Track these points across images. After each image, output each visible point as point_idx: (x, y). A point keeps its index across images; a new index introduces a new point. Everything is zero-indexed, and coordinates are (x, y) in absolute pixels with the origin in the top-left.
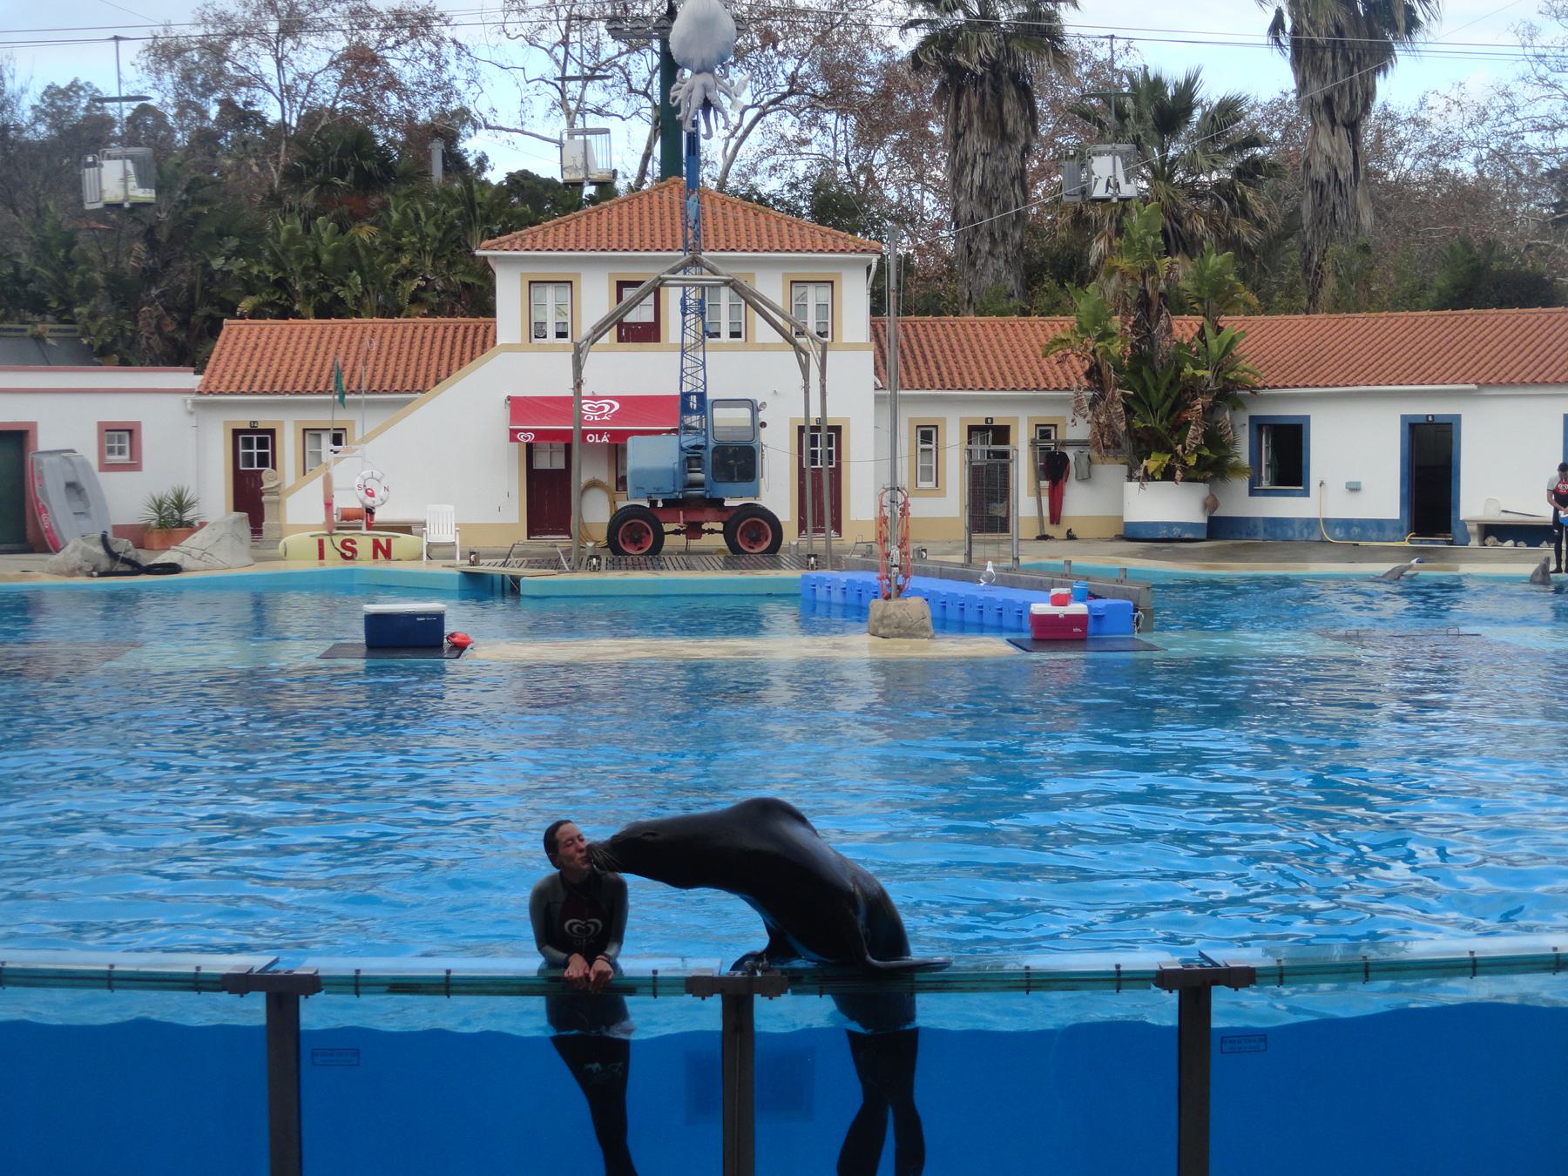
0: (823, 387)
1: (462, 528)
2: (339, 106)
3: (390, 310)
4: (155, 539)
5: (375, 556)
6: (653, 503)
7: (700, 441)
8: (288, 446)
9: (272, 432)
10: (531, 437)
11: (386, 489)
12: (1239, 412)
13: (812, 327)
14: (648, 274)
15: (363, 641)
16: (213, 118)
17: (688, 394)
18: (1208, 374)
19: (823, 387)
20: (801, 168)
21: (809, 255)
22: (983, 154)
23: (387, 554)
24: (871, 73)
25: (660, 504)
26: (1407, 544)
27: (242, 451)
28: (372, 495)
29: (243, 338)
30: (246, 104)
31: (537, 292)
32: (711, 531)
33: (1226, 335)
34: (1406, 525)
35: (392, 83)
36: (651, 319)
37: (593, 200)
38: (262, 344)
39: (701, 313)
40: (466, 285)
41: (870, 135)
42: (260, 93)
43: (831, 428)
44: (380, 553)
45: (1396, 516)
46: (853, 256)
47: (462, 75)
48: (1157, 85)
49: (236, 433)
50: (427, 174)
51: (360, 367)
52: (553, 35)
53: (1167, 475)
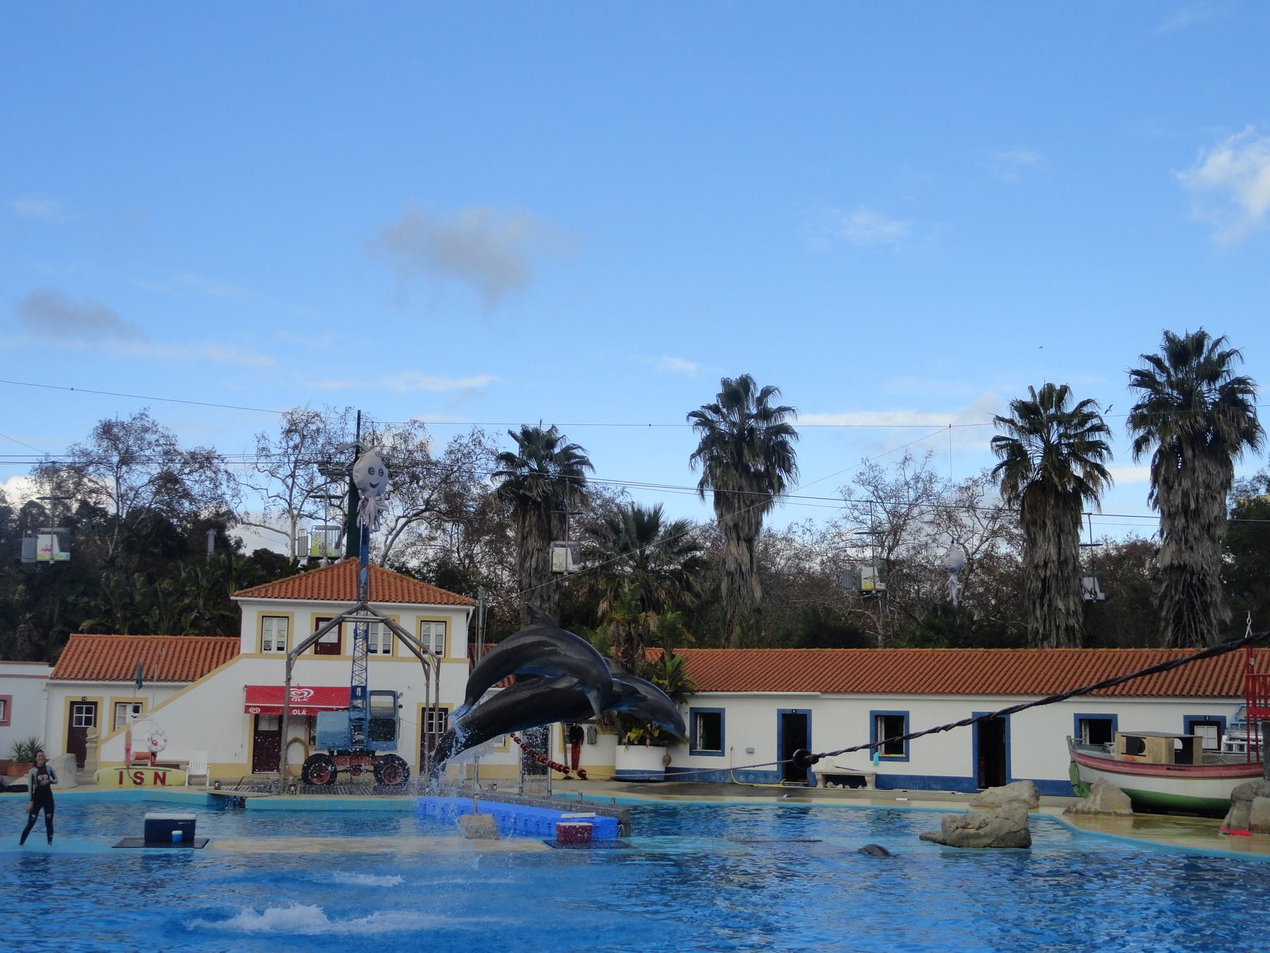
0: (437, 684)
1: (211, 766)
2: (153, 507)
3: (176, 630)
4: (14, 770)
5: (155, 783)
6: (331, 753)
7: (362, 715)
8: (105, 714)
9: (95, 704)
10: (258, 711)
11: (165, 741)
12: (684, 704)
13: (433, 649)
14: (334, 613)
15: (143, 836)
16: (74, 511)
17: (357, 687)
18: (666, 682)
19: (437, 684)
20: (431, 553)
21: (433, 605)
22: (537, 550)
23: (163, 781)
24: (473, 500)
25: (335, 754)
26: (781, 786)
27: (75, 715)
28: (156, 744)
29: (81, 645)
30: (95, 503)
31: (267, 622)
32: (367, 771)
33: (677, 660)
34: (780, 774)
35: (187, 494)
36: (336, 641)
37: (305, 568)
38: (93, 649)
39: (366, 638)
40: (223, 616)
41: (471, 536)
42: (104, 497)
43: (441, 710)
44: (158, 781)
46: (459, 607)
47: (230, 492)
48: (638, 514)
49: (72, 703)
50: (205, 551)
51: (154, 665)
52: (285, 471)
53: (641, 742)
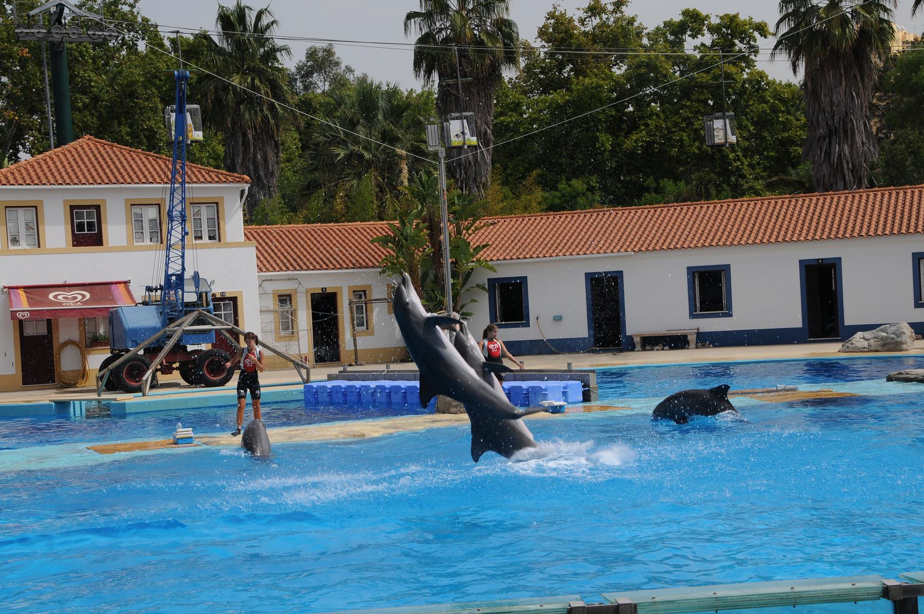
31: (10, 214)
45: (586, 335)
